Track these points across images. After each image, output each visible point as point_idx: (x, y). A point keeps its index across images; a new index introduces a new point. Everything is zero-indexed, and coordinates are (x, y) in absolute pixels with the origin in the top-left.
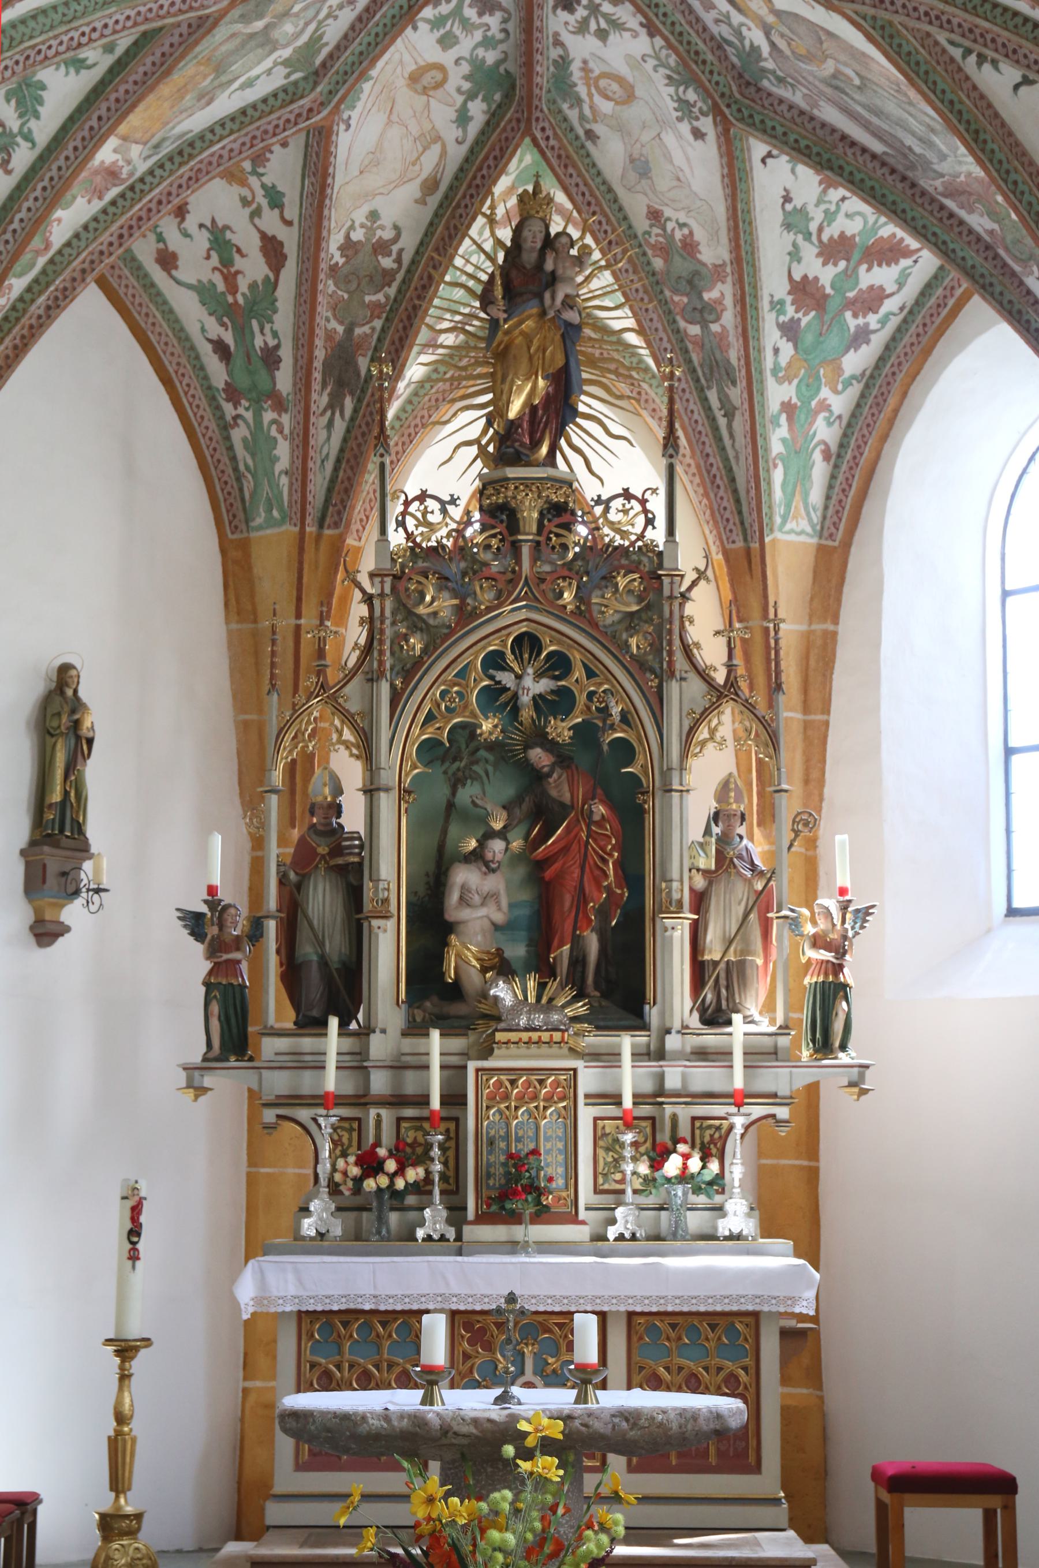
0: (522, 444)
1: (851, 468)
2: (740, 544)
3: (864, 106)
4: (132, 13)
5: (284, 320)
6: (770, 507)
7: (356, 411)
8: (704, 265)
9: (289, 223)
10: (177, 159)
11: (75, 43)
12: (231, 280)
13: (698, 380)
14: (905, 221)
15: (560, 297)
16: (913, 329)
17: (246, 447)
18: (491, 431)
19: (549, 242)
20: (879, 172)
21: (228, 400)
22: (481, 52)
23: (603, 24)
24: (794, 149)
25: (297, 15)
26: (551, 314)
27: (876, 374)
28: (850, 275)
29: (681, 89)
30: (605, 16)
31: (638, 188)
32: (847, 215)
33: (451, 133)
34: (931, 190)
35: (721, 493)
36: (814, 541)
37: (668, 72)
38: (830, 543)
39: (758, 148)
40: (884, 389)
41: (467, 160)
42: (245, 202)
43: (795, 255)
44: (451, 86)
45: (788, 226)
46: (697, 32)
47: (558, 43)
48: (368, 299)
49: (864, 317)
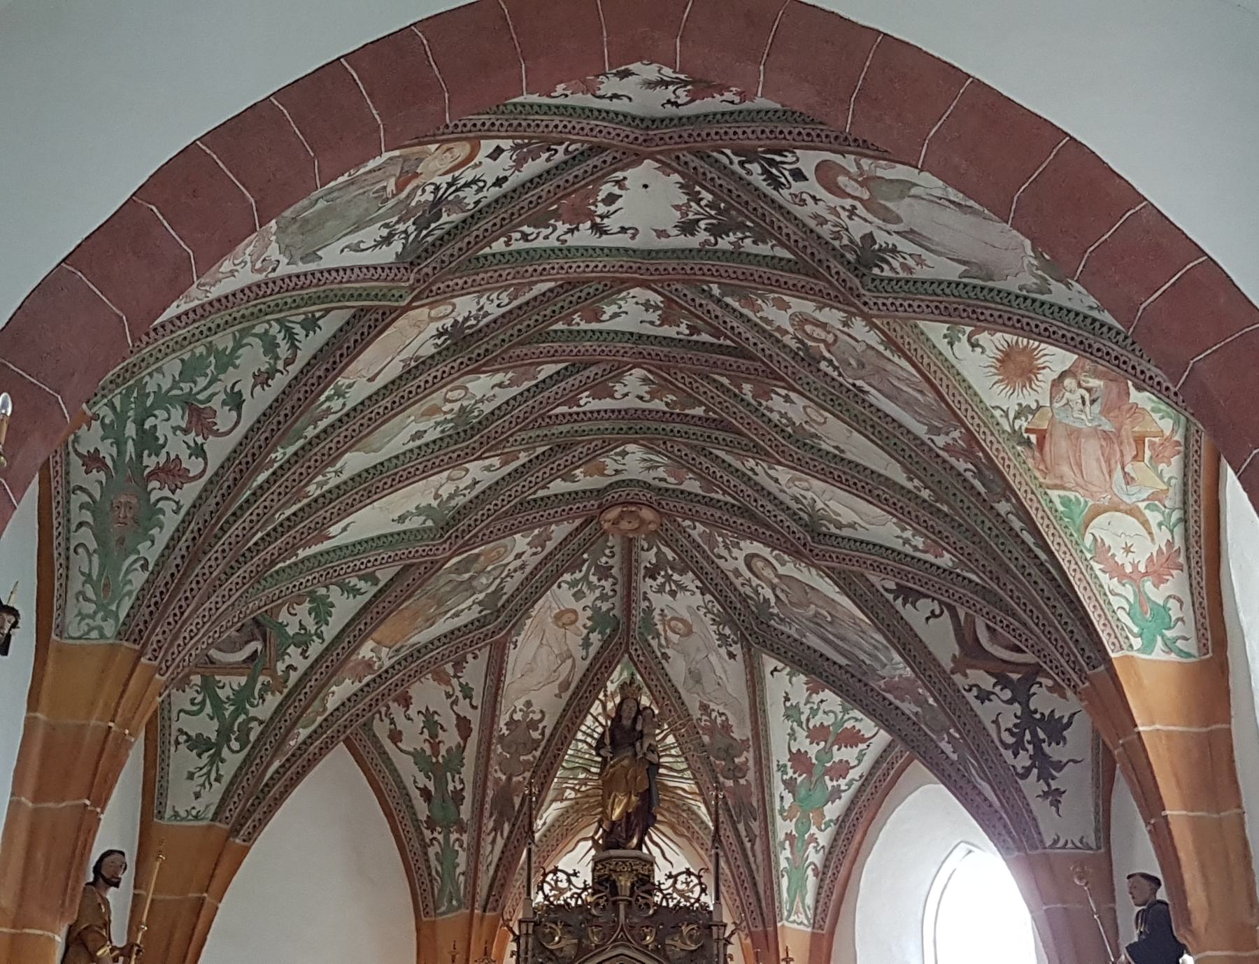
0: (620, 837)
2: (760, 928)
3: (834, 635)
4: (393, 554)
5: (468, 772)
6: (780, 903)
7: (511, 832)
9: (474, 708)
10: (410, 659)
11: (357, 568)
12: (435, 747)
13: (731, 816)
15: (646, 746)
16: (868, 790)
17: (438, 860)
18: (601, 831)
19: (640, 711)
21: (427, 828)
22: (599, 603)
23: (674, 587)
25: (489, 572)
26: (640, 756)
28: (827, 751)
30: (675, 582)
32: (825, 712)
33: (579, 653)
35: (748, 893)
36: (810, 930)
38: (820, 931)
39: (770, 663)
41: (588, 670)
42: (448, 696)
43: (792, 735)
44: (579, 624)
45: (788, 717)
47: (646, 598)
48: (522, 758)
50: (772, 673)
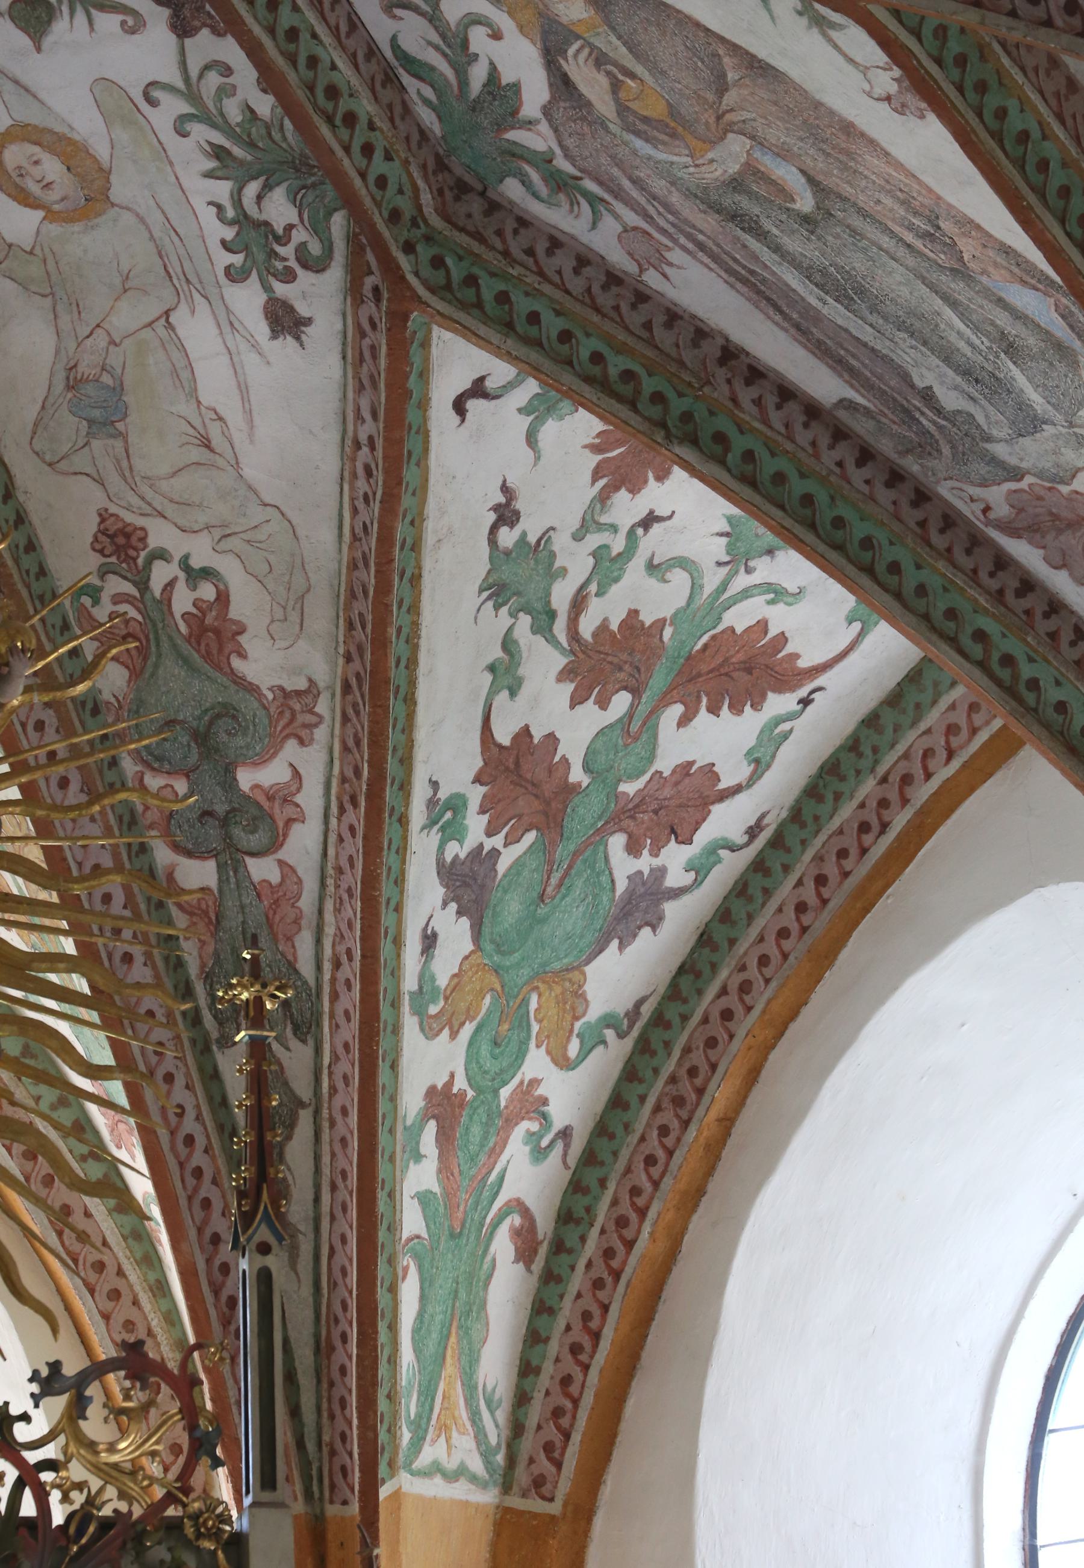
1: (598, 1284)
3: (808, 272)
8: (253, 689)
14: (898, 596)
16: (785, 890)
20: (829, 458)
24: (588, 380)
27: (672, 1013)
29: (252, 189)
31: (81, 462)
32: (652, 567)
34: (970, 511)
36: (488, 1497)
37: (219, 139)
40: (698, 1058)
46: (335, 32)
49: (655, 853)
50: (459, 406)
